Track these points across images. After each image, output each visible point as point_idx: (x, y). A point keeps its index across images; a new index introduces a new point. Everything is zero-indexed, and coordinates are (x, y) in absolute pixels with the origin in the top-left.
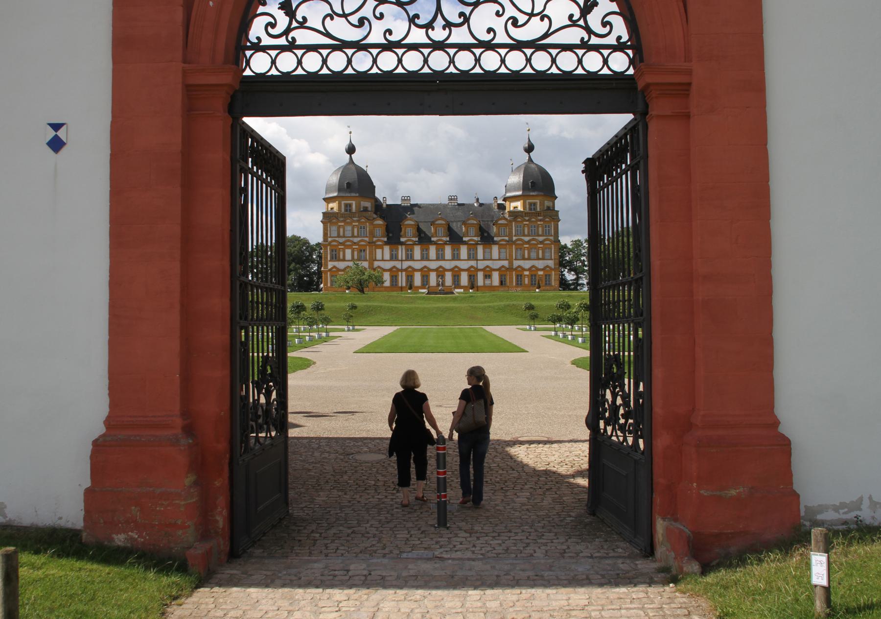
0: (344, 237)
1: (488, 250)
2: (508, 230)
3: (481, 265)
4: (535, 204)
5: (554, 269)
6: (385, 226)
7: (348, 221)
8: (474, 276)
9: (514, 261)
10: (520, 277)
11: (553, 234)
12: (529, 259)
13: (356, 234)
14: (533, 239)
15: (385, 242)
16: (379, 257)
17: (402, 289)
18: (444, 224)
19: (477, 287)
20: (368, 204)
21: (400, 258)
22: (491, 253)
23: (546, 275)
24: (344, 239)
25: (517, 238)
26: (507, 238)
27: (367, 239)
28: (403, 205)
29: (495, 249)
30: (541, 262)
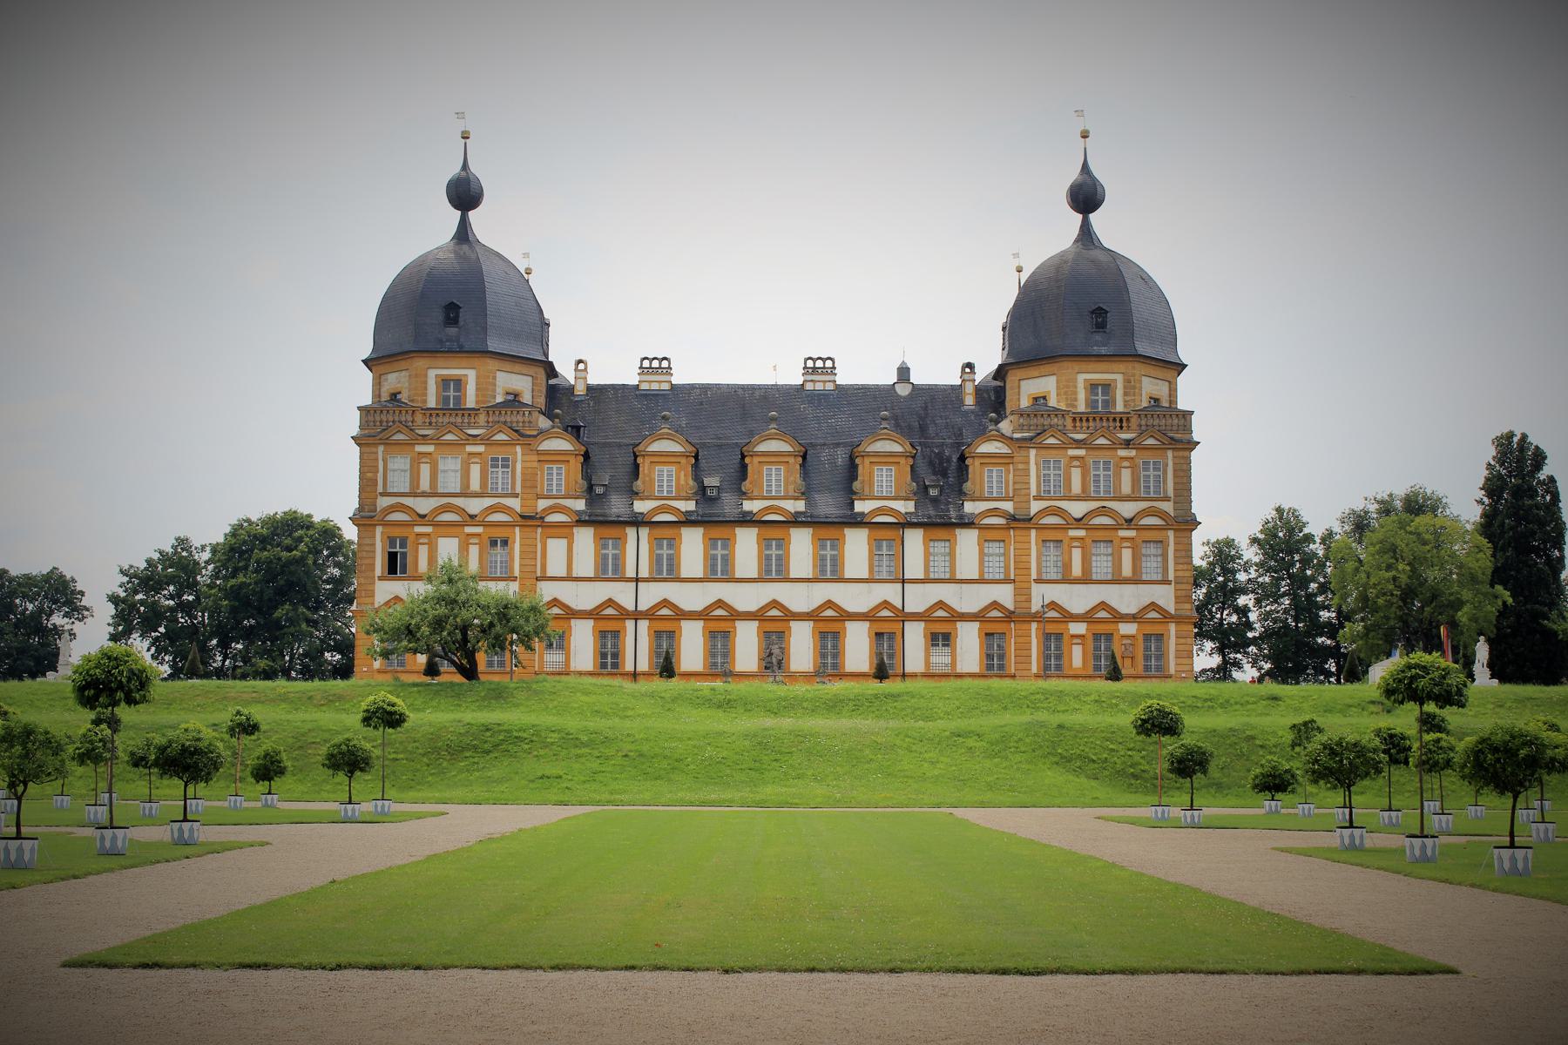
0: (434, 494)
1: (940, 548)
2: (1011, 476)
3: (918, 599)
4: (1107, 387)
5: (1178, 619)
6: (582, 459)
7: (449, 437)
8: (892, 635)
9: (1034, 586)
10: (1054, 642)
11: (1171, 493)
12: (1086, 580)
13: (475, 485)
14: (1103, 511)
15: (578, 513)
16: (556, 566)
17: (635, 675)
18: (789, 454)
19: (904, 675)
20: (522, 384)
21: (631, 573)
22: (952, 555)
23: (1147, 637)
24: (434, 503)
25: (1044, 504)
26: (1008, 506)
27: (515, 504)
28: (644, 386)
29: (967, 541)
30: (1129, 589)
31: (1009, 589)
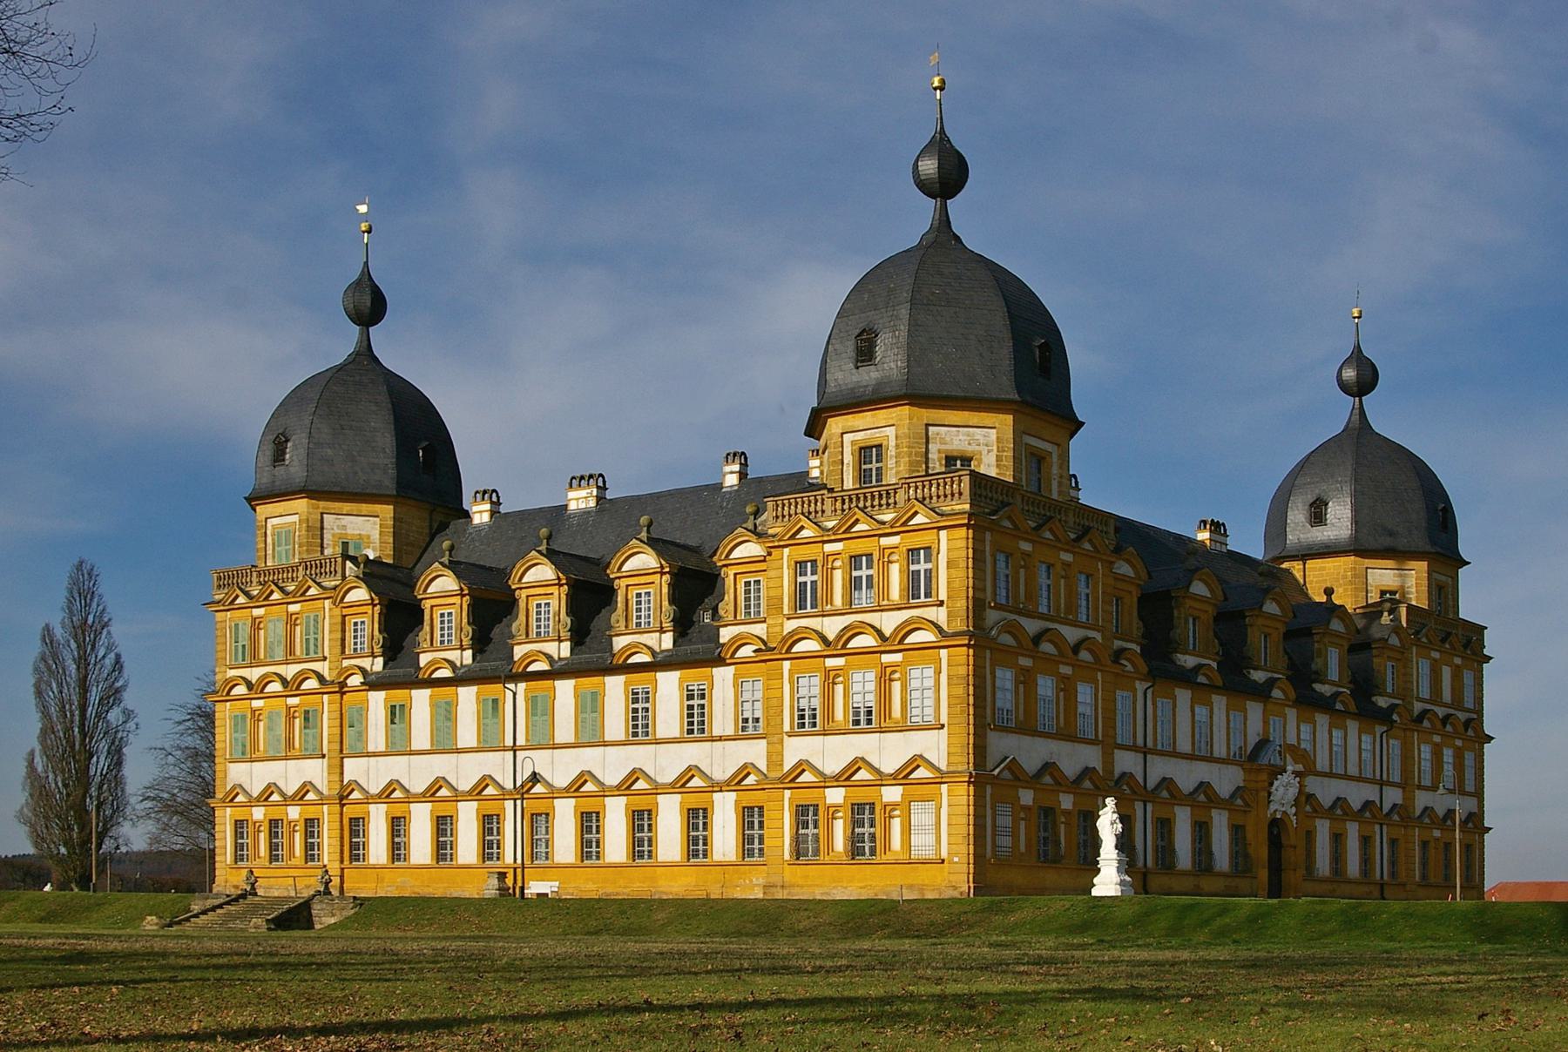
31: (762, 744)
